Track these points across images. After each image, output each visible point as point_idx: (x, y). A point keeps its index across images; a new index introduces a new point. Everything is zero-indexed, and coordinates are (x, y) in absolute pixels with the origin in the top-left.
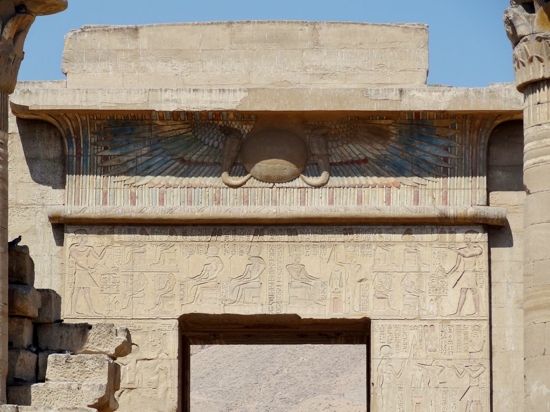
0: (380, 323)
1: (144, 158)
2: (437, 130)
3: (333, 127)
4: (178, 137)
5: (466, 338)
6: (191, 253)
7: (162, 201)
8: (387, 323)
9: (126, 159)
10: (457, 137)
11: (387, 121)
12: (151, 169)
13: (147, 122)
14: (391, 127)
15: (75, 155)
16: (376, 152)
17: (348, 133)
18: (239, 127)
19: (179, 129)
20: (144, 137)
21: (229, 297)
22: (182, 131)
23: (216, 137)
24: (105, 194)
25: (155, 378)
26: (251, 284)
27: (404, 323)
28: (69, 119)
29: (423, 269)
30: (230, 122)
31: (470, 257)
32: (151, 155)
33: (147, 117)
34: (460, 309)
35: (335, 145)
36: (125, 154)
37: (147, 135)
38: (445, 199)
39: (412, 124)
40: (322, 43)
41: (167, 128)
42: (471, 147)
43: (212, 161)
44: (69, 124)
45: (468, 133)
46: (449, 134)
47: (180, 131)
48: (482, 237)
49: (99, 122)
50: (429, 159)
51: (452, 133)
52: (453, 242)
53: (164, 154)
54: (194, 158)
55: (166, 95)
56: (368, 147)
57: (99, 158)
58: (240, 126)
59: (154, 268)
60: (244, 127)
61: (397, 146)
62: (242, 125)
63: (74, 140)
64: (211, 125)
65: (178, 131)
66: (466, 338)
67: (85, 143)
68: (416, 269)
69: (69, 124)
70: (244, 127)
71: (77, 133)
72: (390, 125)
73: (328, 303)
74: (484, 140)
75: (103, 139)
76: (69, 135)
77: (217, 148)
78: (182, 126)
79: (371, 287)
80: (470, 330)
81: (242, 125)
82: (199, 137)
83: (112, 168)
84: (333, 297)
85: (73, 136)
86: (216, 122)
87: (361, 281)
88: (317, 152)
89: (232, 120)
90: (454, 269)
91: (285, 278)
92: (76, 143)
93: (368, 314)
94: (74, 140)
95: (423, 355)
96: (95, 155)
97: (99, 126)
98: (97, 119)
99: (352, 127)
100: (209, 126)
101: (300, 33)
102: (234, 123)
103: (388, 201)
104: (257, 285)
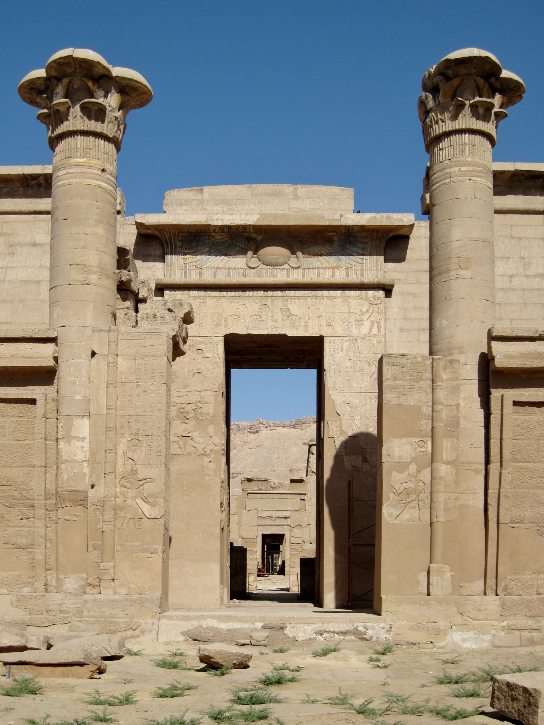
0: (329, 338)
4: (223, 243)
5: (374, 346)
6: (231, 302)
7: (215, 276)
8: (332, 338)
13: (207, 234)
16: (327, 251)
21: (250, 325)
22: (226, 239)
23: (243, 243)
24: (185, 273)
26: (262, 319)
27: (341, 338)
29: (351, 311)
33: (207, 231)
34: (370, 331)
35: (305, 247)
37: (207, 241)
38: (362, 275)
40: (298, 196)
41: (219, 237)
48: (381, 293)
49: (182, 234)
51: (366, 240)
52: (367, 297)
55: (217, 217)
56: (323, 248)
59: (211, 310)
66: (374, 346)
67: (175, 246)
68: (347, 311)
71: (170, 240)
73: (301, 328)
74: (383, 244)
76: (166, 242)
78: (225, 236)
79: (324, 319)
80: (375, 342)
82: (235, 242)
87: (319, 317)
89: (252, 233)
90: (367, 311)
91: (280, 316)
93: (323, 334)
95: (351, 354)
97: (182, 236)
101: (287, 191)
103: (333, 276)
104: (265, 319)
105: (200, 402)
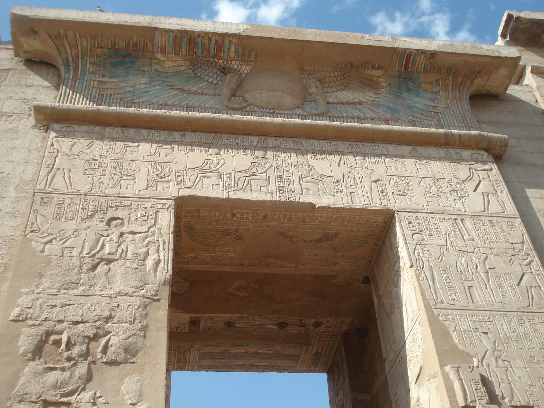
1: (142, 86)
2: (423, 85)
3: (328, 75)
4: (177, 74)
9: (123, 85)
10: (441, 92)
11: (378, 71)
12: (149, 93)
14: (381, 80)
15: (71, 78)
17: (342, 82)
18: (238, 67)
19: (180, 66)
20: (144, 71)
22: (182, 68)
23: (215, 76)
25: (144, 249)
28: (69, 44)
30: (230, 62)
31: (481, 170)
32: (150, 84)
36: (124, 82)
39: (400, 77)
42: (455, 101)
43: (211, 92)
44: (69, 51)
45: (450, 90)
46: (434, 90)
47: (180, 67)
49: (99, 51)
50: (419, 106)
51: (436, 89)
53: (164, 85)
54: (193, 89)
56: (362, 94)
57: (96, 83)
58: (240, 67)
60: (243, 67)
61: (388, 96)
62: (241, 65)
63: (71, 68)
64: (211, 63)
65: (178, 68)
67: (84, 72)
69: (69, 51)
70: (243, 67)
71: (76, 62)
72: (380, 76)
75: (102, 69)
77: (215, 84)
81: (241, 65)
82: (199, 74)
83: (109, 90)
84: (349, 191)
85: (71, 64)
86: (217, 60)
87: (376, 181)
88: (314, 90)
89: (232, 60)
92: (74, 70)
93: (391, 207)
94: (71, 68)
96: (91, 80)
97: (99, 56)
98: (99, 47)
99: (345, 76)
100: (209, 65)
102: (233, 63)
105: (108, 319)
